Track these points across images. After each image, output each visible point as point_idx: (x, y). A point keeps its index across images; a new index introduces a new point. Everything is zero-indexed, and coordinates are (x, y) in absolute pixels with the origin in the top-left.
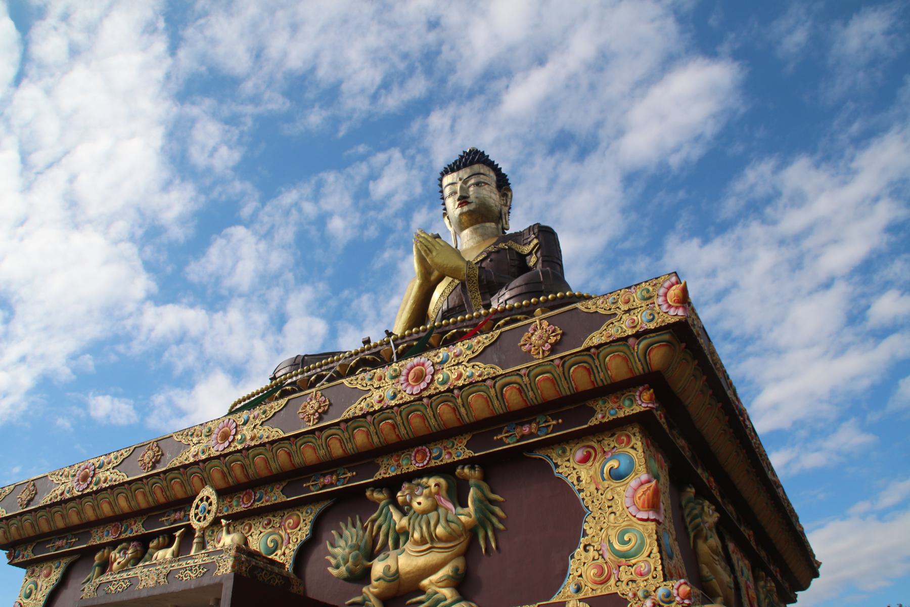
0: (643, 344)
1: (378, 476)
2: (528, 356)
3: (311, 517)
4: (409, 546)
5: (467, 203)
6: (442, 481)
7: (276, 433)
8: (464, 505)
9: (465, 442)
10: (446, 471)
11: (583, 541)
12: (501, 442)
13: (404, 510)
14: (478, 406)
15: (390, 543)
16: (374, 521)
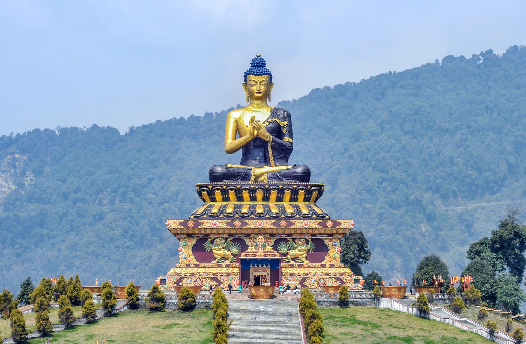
0: (346, 230)
1: (292, 237)
2: (327, 227)
3: (274, 240)
4: (297, 250)
5: (259, 93)
6: (304, 240)
7: (274, 227)
8: (308, 245)
9: (310, 235)
10: (305, 239)
11: (328, 255)
12: (317, 236)
13: (295, 243)
14: (316, 232)
16: (288, 244)
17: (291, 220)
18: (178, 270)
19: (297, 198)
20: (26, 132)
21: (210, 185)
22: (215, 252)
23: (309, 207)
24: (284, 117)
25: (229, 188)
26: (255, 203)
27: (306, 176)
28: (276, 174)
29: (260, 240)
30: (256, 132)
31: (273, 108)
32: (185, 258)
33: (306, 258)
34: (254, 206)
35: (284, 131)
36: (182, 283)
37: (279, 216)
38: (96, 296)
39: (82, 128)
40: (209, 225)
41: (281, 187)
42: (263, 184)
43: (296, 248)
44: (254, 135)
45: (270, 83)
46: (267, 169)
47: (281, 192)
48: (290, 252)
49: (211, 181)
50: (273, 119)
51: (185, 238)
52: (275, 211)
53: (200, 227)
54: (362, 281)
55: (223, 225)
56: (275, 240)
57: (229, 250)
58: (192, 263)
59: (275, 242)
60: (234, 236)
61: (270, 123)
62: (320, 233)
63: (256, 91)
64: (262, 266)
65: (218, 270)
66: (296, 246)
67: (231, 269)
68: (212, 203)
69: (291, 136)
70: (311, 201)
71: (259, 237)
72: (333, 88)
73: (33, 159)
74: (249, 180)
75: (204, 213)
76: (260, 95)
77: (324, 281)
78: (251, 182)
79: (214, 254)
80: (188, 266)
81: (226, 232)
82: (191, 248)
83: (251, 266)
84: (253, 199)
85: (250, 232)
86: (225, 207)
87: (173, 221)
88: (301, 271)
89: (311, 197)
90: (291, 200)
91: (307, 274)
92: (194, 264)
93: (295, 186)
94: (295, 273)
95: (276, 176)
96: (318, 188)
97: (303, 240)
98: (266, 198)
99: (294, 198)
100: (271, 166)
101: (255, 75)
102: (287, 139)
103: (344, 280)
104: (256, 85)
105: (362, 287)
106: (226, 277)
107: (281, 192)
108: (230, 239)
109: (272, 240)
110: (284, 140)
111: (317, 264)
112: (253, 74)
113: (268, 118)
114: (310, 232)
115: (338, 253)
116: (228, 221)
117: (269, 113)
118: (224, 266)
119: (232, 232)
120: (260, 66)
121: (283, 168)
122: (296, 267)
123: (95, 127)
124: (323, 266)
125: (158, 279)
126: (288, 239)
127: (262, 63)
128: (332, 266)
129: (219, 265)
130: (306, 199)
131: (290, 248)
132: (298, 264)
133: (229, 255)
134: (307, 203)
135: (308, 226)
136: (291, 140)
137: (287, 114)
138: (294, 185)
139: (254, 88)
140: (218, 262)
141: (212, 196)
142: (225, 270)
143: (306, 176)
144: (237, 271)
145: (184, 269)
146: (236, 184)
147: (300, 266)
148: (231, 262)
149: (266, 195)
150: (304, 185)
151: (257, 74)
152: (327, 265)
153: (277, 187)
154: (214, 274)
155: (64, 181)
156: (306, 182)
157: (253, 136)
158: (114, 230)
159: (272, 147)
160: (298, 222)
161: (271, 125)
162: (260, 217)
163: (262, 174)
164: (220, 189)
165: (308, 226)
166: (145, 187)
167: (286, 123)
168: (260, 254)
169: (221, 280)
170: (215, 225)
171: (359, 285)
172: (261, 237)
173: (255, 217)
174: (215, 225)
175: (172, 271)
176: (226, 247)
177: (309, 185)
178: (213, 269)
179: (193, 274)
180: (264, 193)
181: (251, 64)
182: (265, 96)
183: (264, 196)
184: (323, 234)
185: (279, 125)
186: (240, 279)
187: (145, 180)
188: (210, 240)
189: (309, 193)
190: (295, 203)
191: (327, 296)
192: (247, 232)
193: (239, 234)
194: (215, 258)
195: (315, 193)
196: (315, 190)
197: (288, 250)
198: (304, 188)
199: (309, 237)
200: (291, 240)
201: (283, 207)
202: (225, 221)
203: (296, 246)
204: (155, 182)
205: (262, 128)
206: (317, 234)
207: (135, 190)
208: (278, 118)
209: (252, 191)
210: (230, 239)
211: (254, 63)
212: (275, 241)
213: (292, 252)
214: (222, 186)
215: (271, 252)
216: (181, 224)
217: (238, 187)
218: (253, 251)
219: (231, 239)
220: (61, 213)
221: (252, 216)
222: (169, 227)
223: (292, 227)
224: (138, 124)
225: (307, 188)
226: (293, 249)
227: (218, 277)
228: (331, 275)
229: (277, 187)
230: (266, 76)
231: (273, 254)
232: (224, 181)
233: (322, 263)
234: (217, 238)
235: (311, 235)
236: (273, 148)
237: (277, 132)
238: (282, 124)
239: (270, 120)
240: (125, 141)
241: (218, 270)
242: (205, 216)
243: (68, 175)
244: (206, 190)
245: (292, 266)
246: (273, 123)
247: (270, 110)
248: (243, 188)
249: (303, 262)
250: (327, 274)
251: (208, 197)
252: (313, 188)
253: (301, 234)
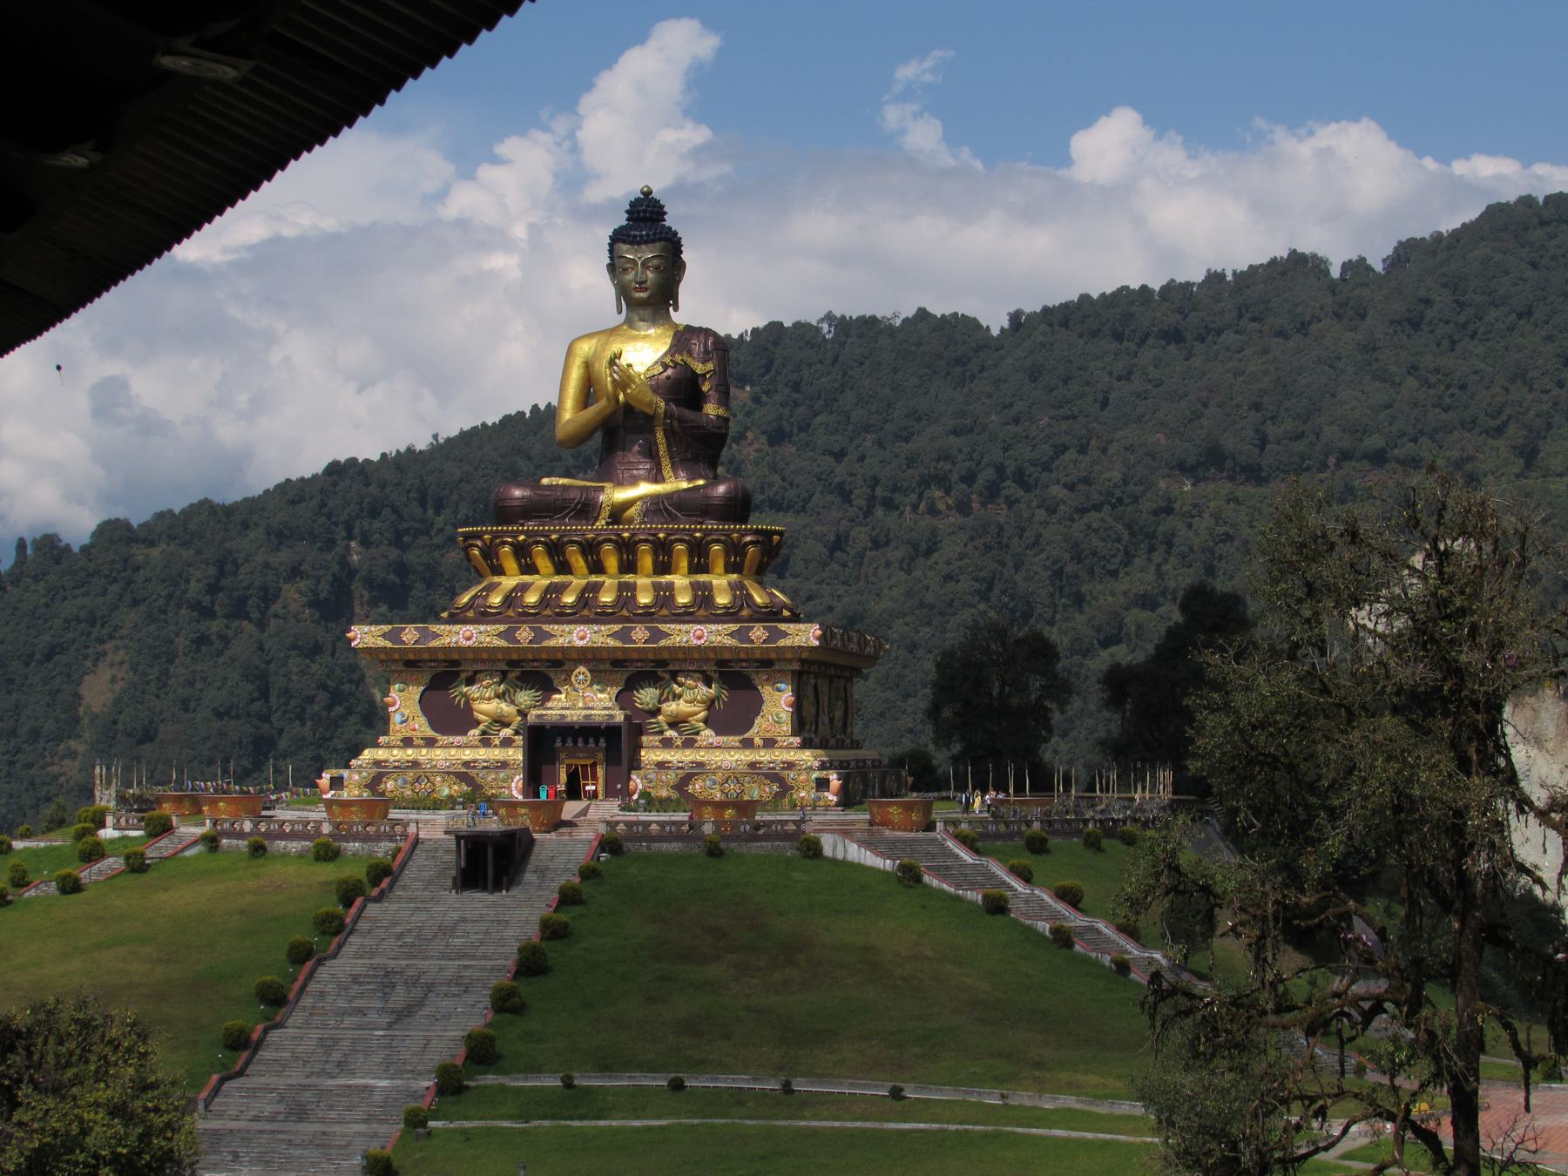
1: (668, 668)
2: (752, 642)
3: (625, 677)
4: (681, 701)
5: (642, 290)
6: (699, 675)
7: (619, 644)
8: (711, 688)
9: (713, 663)
10: (703, 672)
11: (762, 714)
12: (732, 667)
13: (680, 685)
14: (727, 656)
15: (670, 697)
17: (660, 626)
18: (381, 754)
20: (746, 332)
21: (486, 532)
22: (478, 706)
23: (734, 587)
24: (706, 352)
25: (531, 541)
26: (600, 579)
28: (663, 502)
29: (581, 677)
31: (681, 328)
32: (402, 722)
33: (706, 721)
34: (596, 588)
35: (705, 388)
36: (382, 786)
37: (653, 613)
38: (135, 821)
39: (889, 319)
40: (454, 640)
41: (661, 535)
42: (617, 530)
44: (617, 400)
46: (645, 488)
48: (664, 706)
50: (678, 358)
51: (402, 672)
52: (644, 599)
54: (835, 782)
55: (488, 639)
56: (625, 677)
57: (513, 702)
58: (419, 734)
60: (523, 667)
61: (666, 367)
62: (736, 657)
63: (634, 285)
64: (586, 742)
65: (482, 754)
67: (511, 751)
68: (496, 579)
70: (745, 572)
71: (578, 670)
72: (1541, 200)
73: (764, 398)
74: (596, 519)
75: (469, 606)
76: (643, 295)
77: (738, 782)
78: (601, 523)
79: (475, 713)
80: (407, 742)
82: (418, 696)
83: (558, 743)
84: (597, 568)
86: (524, 588)
87: (366, 628)
88: (689, 756)
89: (743, 562)
90: (695, 569)
91: (701, 765)
92: (422, 739)
93: (698, 535)
94: (669, 762)
95: (656, 507)
96: (761, 539)
97: (696, 675)
98: (629, 566)
99: (699, 565)
100: (663, 480)
101: (631, 243)
102: (711, 409)
103: (790, 782)
104: (633, 269)
105: (835, 799)
106: (493, 772)
108: (514, 675)
109: (619, 675)
110: (705, 411)
111: (731, 738)
112: (624, 242)
113: (665, 354)
114: (712, 655)
115: (787, 709)
116: (502, 628)
117: (669, 341)
118: (497, 742)
119: (515, 657)
120: (645, 220)
122: (677, 747)
123: (922, 314)
124: (748, 744)
125: (324, 775)
126: (660, 673)
127: (652, 212)
128: (770, 743)
129: (486, 742)
130: (730, 568)
131: (665, 695)
132: (684, 738)
133: (510, 714)
134: (735, 576)
135: (702, 641)
136: (721, 412)
137: (714, 343)
138: (696, 530)
139: (630, 276)
140: (484, 733)
141: (492, 562)
142: (496, 754)
144: (516, 755)
145: (395, 752)
146: (549, 530)
147: (689, 744)
148: (517, 733)
149: (625, 556)
150: (723, 530)
151: (635, 242)
152: (758, 741)
153: (651, 538)
154: (466, 764)
155: (839, 456)
156: (735, 521)
157: (613, 403)
158: (958, 581)
159: (665, 431)
160: (680, 630)
161: (670, 372)
162: (603, 617)
163: (629, 504)
164: (511, 544)
165: (702, 641)
166: (1047, 467)
167: (710, 366)
168: (575, 716)
169: (479, 780)
170: (469, 639)
171: (826, 794)
172: (582, 669)
173: (592, 616)
174: (469, 639)
175: (367, 755)
176: (504, 693)
177: (734, 530)
178: (468, 752)
179: (415, 764)
181: (627, 212)
184: (745, 661)
185: (693, 373)
186: (523, 779)
187: (1047, 448)
188: (463, 676)
190: (702, 578)
191: (673, 829)
192: (552, 657)
193: (534, 661)
194: (478, 723)
196: (751, 543)
197: (660, 702)
198: (723, 538)
199: (710, 668)
200: (667, 676)
201: (708, 587)
202: (494, 627)
204: (1072, 454)
205: (634, 382)
206: (731, 661)
207: (1021, 478)
208: (690, 353)
209: (591, 550)
210: (514, 675)
211: (639, 212)
212: (629, 678)
213: (671, 707)
214: (515, 534)
215: (605, 708)
216: (384, 636)
217: (554, 537)
218: (560, 705)
219: (518, 674)
220: (832, 538)
221: (586, 612)
222: (356, 643)
223: (663, 643)
224: (1032, 306)
225: (731, 539)
226: (674, 700)
227: (473, 772)
228: (760, 768)
229: (651, 538)
230: (658, 244)
231: (607, 712)
232: (521, 521)
233: (745, 736)
234: (481, 671)
235: (716, 664)
236: (670, 434)
238: (699, 368)
239: (667, 360)
240: (997, 350)
241: (482, 754)
242: (470, 614)
243: (852, 439)
244: (477, 546)
245: (667, 744)
246: (674, 367)
247: (671, 333)
248: (566, 539)
249: (697, 733)
250: (752, 765)
251: (484, 564)
252: (748, 539)
253: (692, 661)
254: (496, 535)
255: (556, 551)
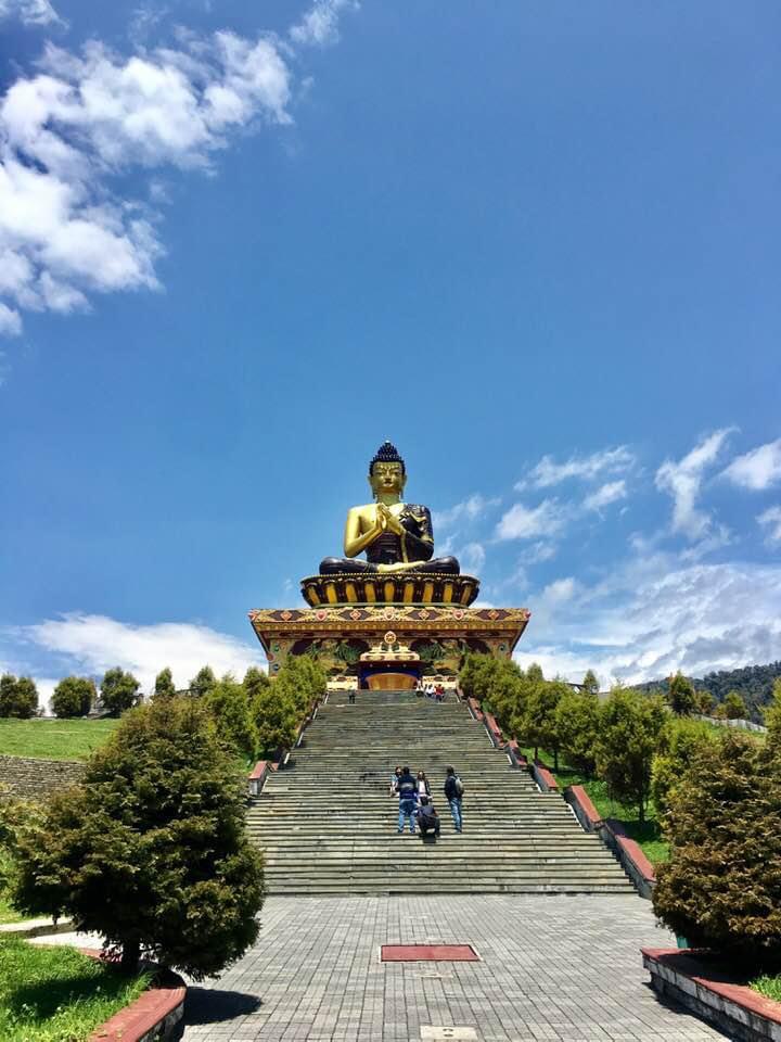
10: (457, 639)
19: (442, 597)
24: (421, 512)
27: (453, 567)
30: (384, 524)
43: (444, 654)
45: (402, 462)
47: (419, 586)
49: (321, 573)
53: (300, 620)
57: (343, 658)
59: (413, 644)
66: (443, 651)
69: (431, 535)
81: (339, 628)
85: (375, 627)
95: (409, 570)
99: (437, 598)
102: (425, 538)
107: (419, 586)
119: (348, 628)
121: (422, 562)
126: (432, 641)
134: (457, 604)
143: (453, 567)
164: (335, 584)
167: (424, 518)
168: (390, 656)
172: (391, 632)
180: (396, 589)
182: (397, 490)
183: (395, 594)
188: (314, 642)
189: (459, 589)
193: (358, 631)
195: (467, 592)
203: (443, 651)
209: (379, 586)
214: (336, 578)
219: (347, 641)
237: (412, 526)
238: (419, 520)
252: (465, 582)
254: (324, 579)
255: (359, 587)
